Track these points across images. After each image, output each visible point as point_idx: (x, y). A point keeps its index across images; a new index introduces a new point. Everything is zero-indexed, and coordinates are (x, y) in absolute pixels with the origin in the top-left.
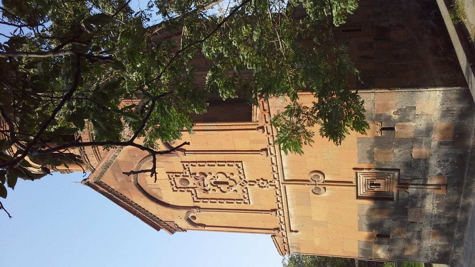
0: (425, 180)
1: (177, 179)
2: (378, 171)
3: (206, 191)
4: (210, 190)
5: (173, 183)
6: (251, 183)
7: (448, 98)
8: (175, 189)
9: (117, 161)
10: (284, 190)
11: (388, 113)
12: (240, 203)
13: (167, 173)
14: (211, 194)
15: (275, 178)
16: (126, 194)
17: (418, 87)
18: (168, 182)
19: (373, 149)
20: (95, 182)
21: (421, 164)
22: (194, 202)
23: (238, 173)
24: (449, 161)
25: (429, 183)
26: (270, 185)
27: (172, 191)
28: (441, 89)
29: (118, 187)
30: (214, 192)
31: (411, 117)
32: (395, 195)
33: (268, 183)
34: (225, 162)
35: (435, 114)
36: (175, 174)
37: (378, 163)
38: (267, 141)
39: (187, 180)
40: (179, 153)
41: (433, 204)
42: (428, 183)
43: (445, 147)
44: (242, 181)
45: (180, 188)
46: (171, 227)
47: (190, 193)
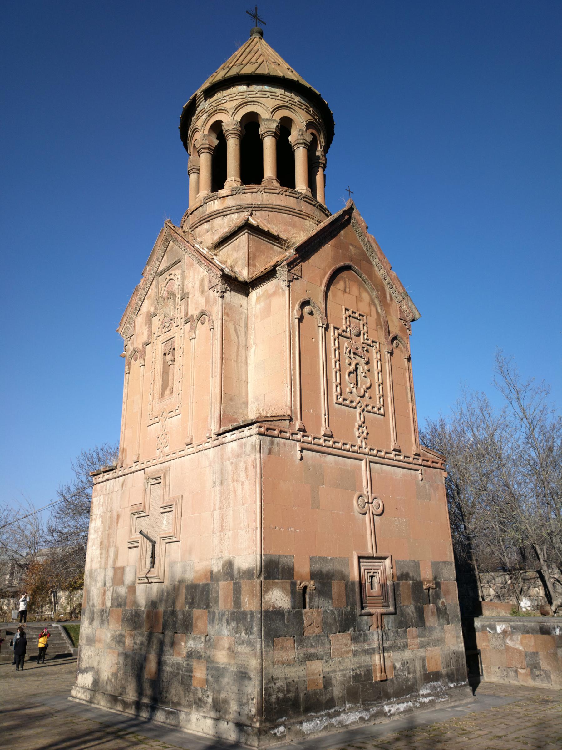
5: (354, 315)
6: (362, 416)
7: (459, 657)
10: (359, 457)
11: (442, 594)
21: (402, 640)
24: (409, 676)
26: (362, 441)
28: (464, 648)
29: (342, 238)
33: (365, 438)
37: (398, 584)
38: (408, 455)
41: (360, 667)
42: (386, 654)
43: (421, 666)
47: (344, 328)
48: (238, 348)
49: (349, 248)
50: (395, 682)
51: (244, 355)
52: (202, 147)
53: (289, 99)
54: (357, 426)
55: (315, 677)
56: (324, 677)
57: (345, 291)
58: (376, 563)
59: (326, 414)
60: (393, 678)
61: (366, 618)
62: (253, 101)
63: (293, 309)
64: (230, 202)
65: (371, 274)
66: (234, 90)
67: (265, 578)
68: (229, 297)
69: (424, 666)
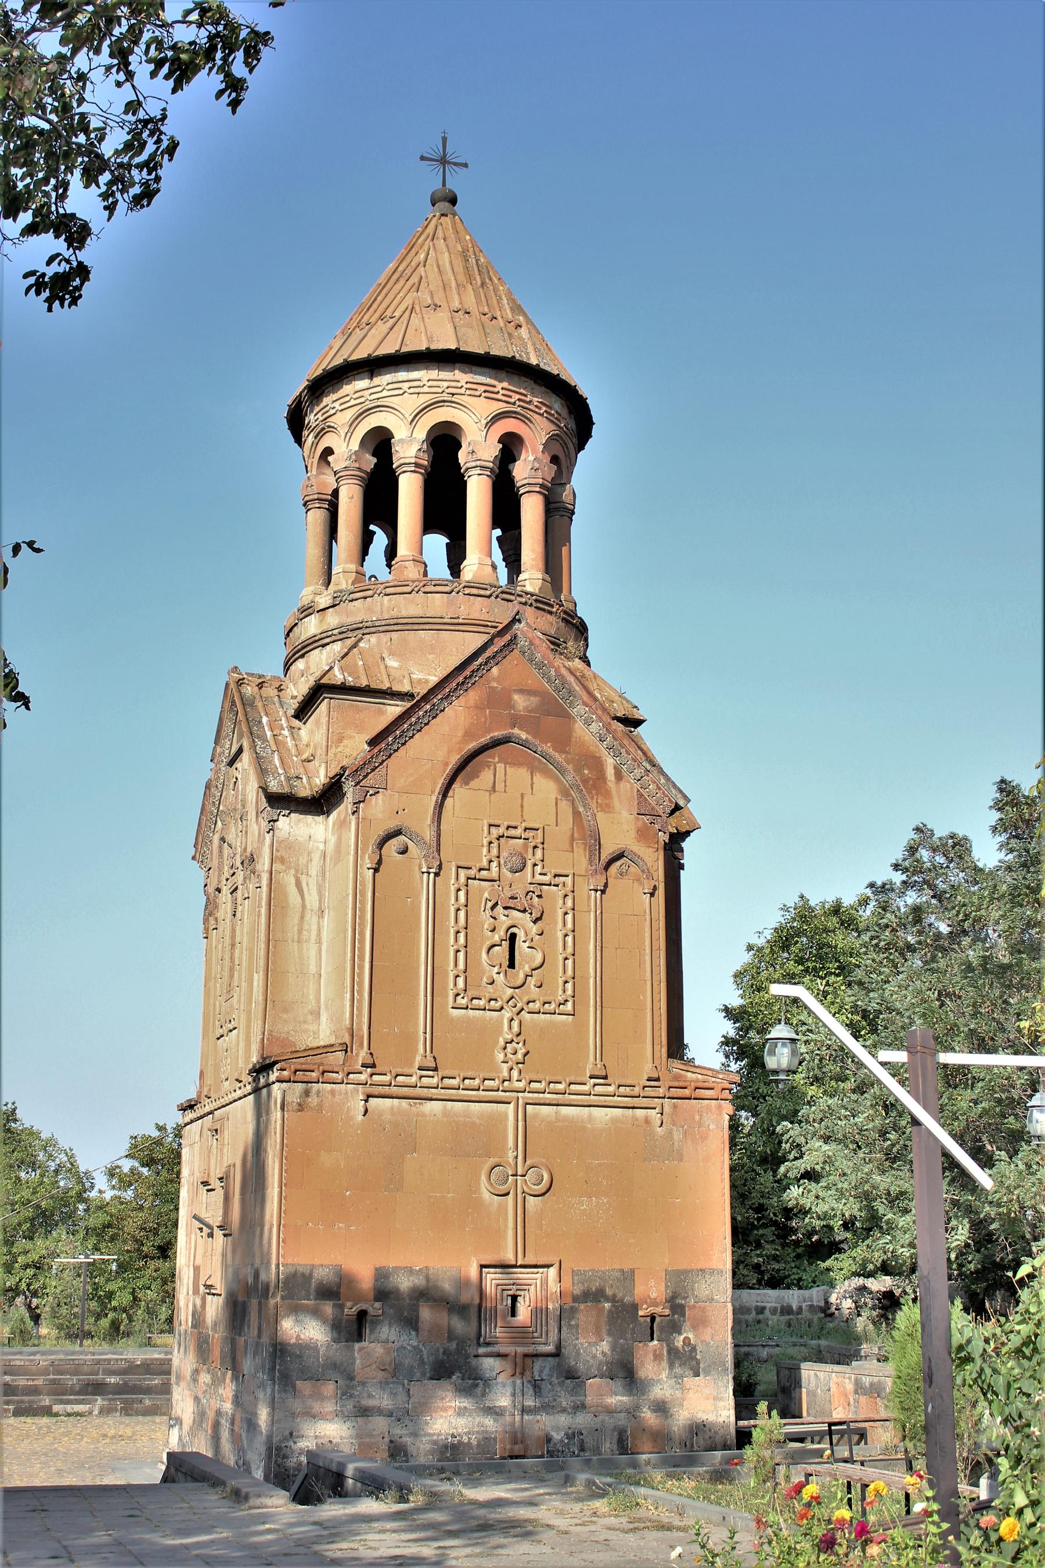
1: (525, 847)
3: (493, 908)
5: (512, 832)
6: (515, 1024)
8: (495, 832)
11: (687, 1326)
16: (472, 696)
19: (607, 1300)
21: (573, 1398)
29: (495, 684)
31: (678, 1370)
37: (573, 1311)
38: (629, 1082)
43: (615, 1440)
46: (368, 774)
47: (485, 863)
48: (302, 917)
49: (510, 699)
51: (314, 927)
52: (306, 499)
53: (446, 384)
54: (502, 1042)
55: (373, 1440)
56: (391, 1441)
58: (523, 1275)
59: (428, 1031)
62: (379, 406)
63: (363, 853)
64: (333, 619)
65: (564, 741)
66: (347, 389)
67: (283, 1298)
68: (287, 828)
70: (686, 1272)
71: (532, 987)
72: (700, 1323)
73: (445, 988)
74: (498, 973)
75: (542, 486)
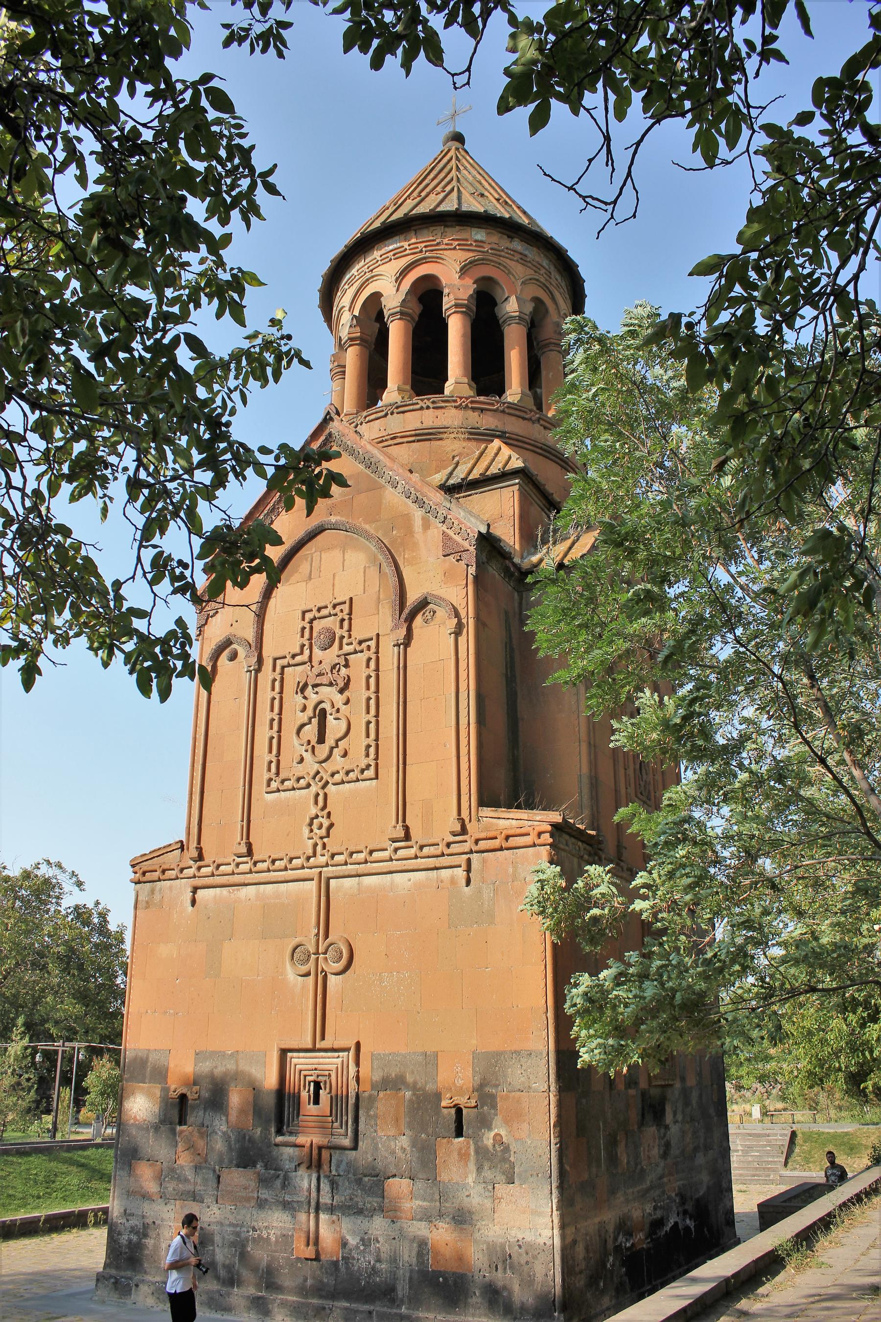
0: (331, 1210)
2: (352, 1101)
3: (303, 690)
4: (305, 698)
5: (324, 612)
6: (321, 799)
7: (535, 1257)
8: (309, 616)
9: (381, 487)
10: (302, 877)
11: (498, 1121)
12: (269, 770)
13: (351, 599)
14: (293, 700)
15: (332, 856)
17: (561, 1187)
18: (327, 600)
19: (407, 1086)
20: (330, 434)
21: (370, 1199)
22: (275, 660)
23: (347, 768)
24: (378, 1265)
25: (323, 1217)
26: (315, 845)
27: (305, 608)
28: (557, 1241)
30: (299, 707)
32: (292, 1139)
33: (322, 838)
34: (377, 739)
35: (497, 1228)
36: (346, 617)
37: (372, 1099)
38: (431, 841)
39: (331, 646)
40: (403, 631)
43: (414, 1253)
44: (326, 777)
45: (311, 628)
47: (298, 650)
50: (343, 1269)
54: (308, 820)
57: (310, 578)
60: (338, 1261)
61: (290, 1150)
69: (420, 1255)
70: (498, 1054)
71: (338, 758)
72: (514, 1117)
73: (262, 775)
74: (306, 751)
75: (456, 306)
